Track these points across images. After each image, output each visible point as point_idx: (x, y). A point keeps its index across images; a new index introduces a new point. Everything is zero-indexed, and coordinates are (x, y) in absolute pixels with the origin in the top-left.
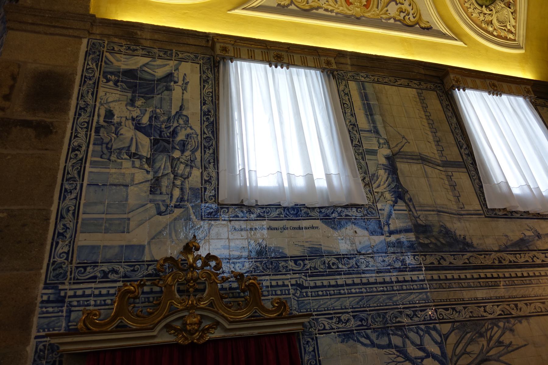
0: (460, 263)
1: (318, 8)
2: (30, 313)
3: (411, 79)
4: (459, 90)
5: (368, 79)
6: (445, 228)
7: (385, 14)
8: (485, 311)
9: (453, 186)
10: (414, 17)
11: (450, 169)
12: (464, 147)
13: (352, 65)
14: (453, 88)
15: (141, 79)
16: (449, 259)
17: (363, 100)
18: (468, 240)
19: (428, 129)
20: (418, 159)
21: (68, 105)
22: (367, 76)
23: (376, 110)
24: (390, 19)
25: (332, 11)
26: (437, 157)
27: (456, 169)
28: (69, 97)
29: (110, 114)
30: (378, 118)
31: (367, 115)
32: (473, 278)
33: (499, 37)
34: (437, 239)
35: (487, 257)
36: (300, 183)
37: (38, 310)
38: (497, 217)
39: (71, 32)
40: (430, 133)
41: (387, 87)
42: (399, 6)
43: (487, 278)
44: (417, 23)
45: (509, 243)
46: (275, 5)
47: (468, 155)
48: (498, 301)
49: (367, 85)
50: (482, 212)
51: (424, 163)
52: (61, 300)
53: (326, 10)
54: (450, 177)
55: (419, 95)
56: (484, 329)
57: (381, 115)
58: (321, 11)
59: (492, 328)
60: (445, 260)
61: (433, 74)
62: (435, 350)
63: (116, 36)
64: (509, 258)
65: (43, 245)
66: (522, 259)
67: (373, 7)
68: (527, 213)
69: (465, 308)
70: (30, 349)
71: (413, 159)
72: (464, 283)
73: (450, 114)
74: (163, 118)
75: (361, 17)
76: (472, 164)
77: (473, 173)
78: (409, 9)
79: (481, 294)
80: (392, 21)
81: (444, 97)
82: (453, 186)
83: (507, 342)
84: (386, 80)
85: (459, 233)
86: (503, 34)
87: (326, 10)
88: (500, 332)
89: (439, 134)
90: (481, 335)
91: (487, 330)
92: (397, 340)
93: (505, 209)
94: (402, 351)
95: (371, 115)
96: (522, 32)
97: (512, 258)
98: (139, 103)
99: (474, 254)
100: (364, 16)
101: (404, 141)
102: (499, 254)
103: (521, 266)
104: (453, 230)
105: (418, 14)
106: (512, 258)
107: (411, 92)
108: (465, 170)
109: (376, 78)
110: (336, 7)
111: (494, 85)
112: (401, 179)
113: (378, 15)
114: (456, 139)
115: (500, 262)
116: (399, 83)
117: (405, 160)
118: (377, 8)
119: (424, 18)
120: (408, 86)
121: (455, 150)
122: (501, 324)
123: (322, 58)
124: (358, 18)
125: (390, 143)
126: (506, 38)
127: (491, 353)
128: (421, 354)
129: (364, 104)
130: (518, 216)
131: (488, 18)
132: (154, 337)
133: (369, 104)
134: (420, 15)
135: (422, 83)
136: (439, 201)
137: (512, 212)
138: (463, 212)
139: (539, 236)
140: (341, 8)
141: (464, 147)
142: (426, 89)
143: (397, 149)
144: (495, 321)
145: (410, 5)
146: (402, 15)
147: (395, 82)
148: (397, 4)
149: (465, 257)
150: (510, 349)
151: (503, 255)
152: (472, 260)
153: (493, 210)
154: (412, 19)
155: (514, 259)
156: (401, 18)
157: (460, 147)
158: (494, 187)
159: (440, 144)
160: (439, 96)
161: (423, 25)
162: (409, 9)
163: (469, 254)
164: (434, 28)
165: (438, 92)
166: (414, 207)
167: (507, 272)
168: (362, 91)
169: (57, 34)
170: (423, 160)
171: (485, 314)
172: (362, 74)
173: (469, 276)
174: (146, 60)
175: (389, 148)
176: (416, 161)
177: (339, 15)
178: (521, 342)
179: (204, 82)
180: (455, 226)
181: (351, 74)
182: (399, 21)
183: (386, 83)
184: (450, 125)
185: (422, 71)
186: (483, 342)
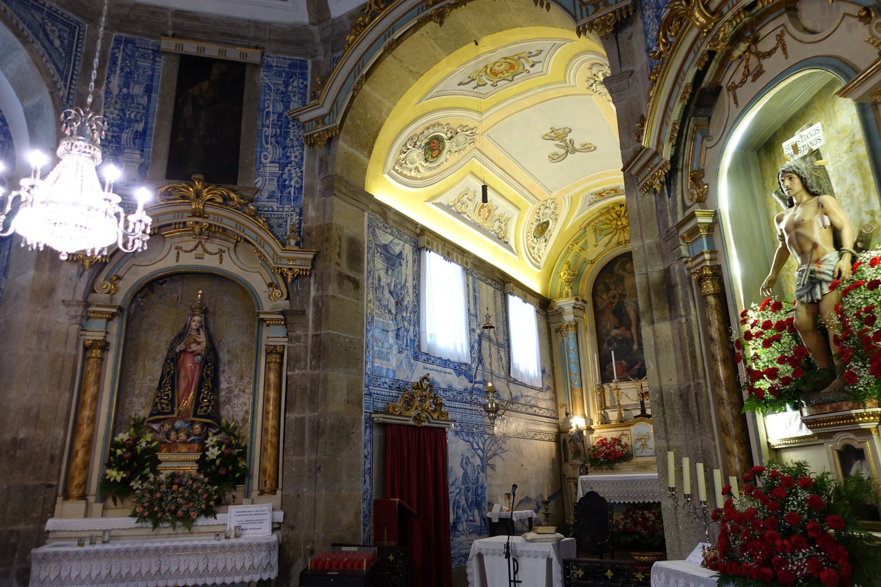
1: (465, 213)
2: (361, 399)
3: (493, 280)
15: (390, 254)
21: (363, 267)
23: (478, 303)
28: (363, 262)
29: (380, 280)
30: (478, 306)
33: (534, 258)
36: (451, 348)
37: (364, 399)
39: (360, 205)
46: (446, 204)
52: (370, 394)
53: (468, 216)
55: (495, 292)
58: (465, 216)
61: (502, 278)
62: (481, 446)
63: (378, 213)
65: (362, 362)
70: (363, 417)
74: (399, 287)
80: (493, 233)
84: (483, 278)
86: (537, 257)
87: (468, 216)
92: (471, 439)
94: (472, 445)
96: (544, 258)
98: (390, 272)
103: (513, 411)
105: (506, 233)
107: (491, 289)
111: (525, 296)
120: (491, 285)
123: (465, 259)
126: (536, 260)
128: (477, 447)
131: (534, 245)
132: (408, 421)
139: (522, 396)
161: (506, 240)
169: (356, 207)
174: (391, 238)
179: (414, 261)
183: (483, 281)
185: (499, 276)
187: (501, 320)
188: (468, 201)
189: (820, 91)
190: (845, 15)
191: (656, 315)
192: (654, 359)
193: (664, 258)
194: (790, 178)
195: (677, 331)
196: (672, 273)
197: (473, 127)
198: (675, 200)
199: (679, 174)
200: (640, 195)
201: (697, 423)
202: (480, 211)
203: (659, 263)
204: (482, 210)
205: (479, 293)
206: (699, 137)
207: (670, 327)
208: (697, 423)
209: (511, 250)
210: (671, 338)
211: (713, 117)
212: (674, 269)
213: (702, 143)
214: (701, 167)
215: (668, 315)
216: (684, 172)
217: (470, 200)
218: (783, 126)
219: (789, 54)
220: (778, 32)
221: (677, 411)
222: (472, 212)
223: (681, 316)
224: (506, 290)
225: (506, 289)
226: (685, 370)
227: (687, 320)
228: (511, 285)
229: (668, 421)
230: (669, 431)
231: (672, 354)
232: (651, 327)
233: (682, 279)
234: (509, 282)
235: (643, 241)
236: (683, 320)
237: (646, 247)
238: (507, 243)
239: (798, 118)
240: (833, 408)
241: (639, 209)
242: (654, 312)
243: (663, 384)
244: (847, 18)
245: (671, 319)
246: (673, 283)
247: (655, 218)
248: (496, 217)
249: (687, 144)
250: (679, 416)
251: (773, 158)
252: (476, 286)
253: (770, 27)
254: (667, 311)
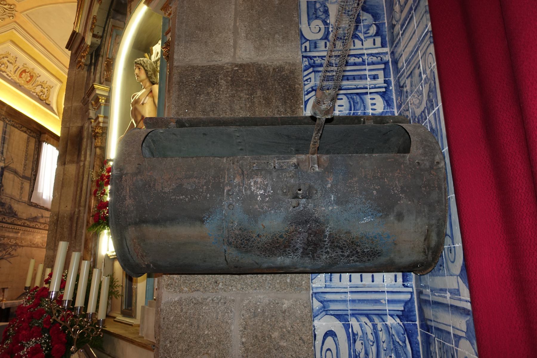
0: (9, 221)
3: (28, 129)
4: (46, 143)
5: (9, 123)
6: (11, 206)
7: (34, 89)
8: (10, 241)
9: (22, 188)
10: (46, 97)
11: (24, 180)
12: (34, 171)
13: (6, 112)
14: (44, 141)
16: (7, 219)
17: (3, 134)
18: (17, 213)
19: (24, 158)
20: (13, 172)
22: (10, 121)
23: (7, 142)
24: (34, 93)
25: (10, 77)
26: (22, 173)
27: (26, 181)
30: (6, 145)
31: (1, 143)
32: (11, 228)
34: (6, 210)
35: (20, 221)
38: (32, 206)
40: (24, 160)
41: (16, 130)
42: (42, 89)
43: (16, 229)
44: (45, 100)
45: (31, 217)
47: (34, 175)
48: (16, 239)
49: (8, 125)
50: (27, 202)
51: (16, 174)
53: (8, 75)
54: (22, 183)
55: (28, 138)
56: (6, 248)
57: (8, 145)
58: (4, 74)
59: (9, 248)
60: (5, 219)
61: (39, 129)
64: (28, 223)
66: (32, 224)
67: (30, 84)
68: (43, 207)
69: (4, 239)
71: (12, 171)
72: (8, 230)
73: (36, 153)
75: (22, 86)
76: (34, 180)
77: (32, 184)
78: (46, 92)
79: (11, 235)
80: (35, 94)
81: (37, 143)
82: (22, 188)
83: (12, 254)
84: (17, 126)
85: (15, 209)
87: (8, 75)
88: (11, 250)
89: (27, 162)
90: (5, 250)
91: (7, 249)
93: (36, 204)
95: (4, 143)
97: (28, 223)
99: (16, 219)
100: (23, 86)
101: (12, 161)
102: (25, 221)
104: (13, 207)
105: (48, 97)
106: (28, 223)
107: (25, 136)
108: (29, 182)
109: (14, 123)
110: (14, 75)
112: (3, 180)
113: (30, 88)
114: (33, 166)
115: (24, 224)
116: (22, 129)
117: (8, 171)
118: (32, 85)
119: (50, 99)
120: (25, 132)
121: (30, 171)
122: (13, 247)
124: (20, 86)
125: (6, 161)
127: (5, 257)
129: (2, 136)
130: (39, 207)
133: (4, 137)
134: (49, 97)
135: (32, 132)
136: (13, 194)
137: (38, 205)
138: (20, 201)
139: (42, 217)
140: (15, 77)
141: (34, 171)
142: (32, 136)
143: (7, 165)
144: (11, 246)
145: (47, 91)
146: (41, 93)
147: (20, 128)
148: (42, 87)
149: (13, 219)
150: (12, 256)
151: (27, 222)
152: (14, 221)
153: (32, 202)
154: (44, 97)
155: (29, 224)
156: (40, 94)
157: (32, 170)
158: (37, 193)
159: (26, 167)
160: (36, 142)
161: (47, 102)
162: (46, 92)
163: (14, 219)
164: (51, 105)
165: (37, 139)
166: (3, 194)
167: (24, 228)
168: (5, 129)
170: (15, 172)
171: (9, 243)
172: (8, 119)
173: (10, 227)
175: (4, 163)
176: (12, 172)
177: (12, 80)
178: (17, 255)
180: (15, 206)
181: (2, 117)
182: (38, 95)
183: (16, 127)
184: (34, 158)
186: (4, 252)
187: (31, 159)
188: (8, 64)
197: (11, 3)
202: (21, 74)
204: (24, 74)
205: (10, 136)
209: (52, 110)
217: (11, 63)
222: (12, 73)
224: (41, 139)
225: (41, 138)
228: (46, 135)
234: (45, 133)
235: (72, 104)
237: (73, 108)
238: (49, 105)
241: (75, 80)
247: (84, 89)
248: (39, 83)
249: (107, 38)
252: (8, 130)
254: (76, 156)
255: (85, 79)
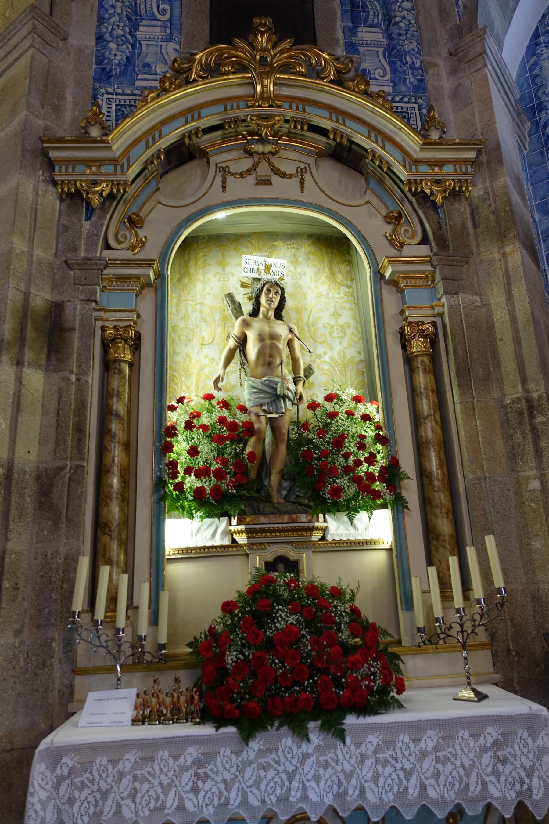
189: (260, 233)
190: (368, 202)
191: (29, 355)
192: (9, 416)
193: (55, 286)
194: (277, 293)
195: (55, 388)
196: (68, 311)
198: (98, 227)
199: (115, 203)
200: (42, 187)
201: (64, 519)
203: (47, 289)
206: (153, 186)
207: (42, 380)
208: (64, 519)
210: (41, 394)
211: (170, 176)
212: (75, 309)
213: (154, 193)
214: (142, 214)
215: (43, 362)
216: (119, 206)
218: (208, 236)
219: (305, 190)
220: (302, 166)
221: (28, 499)
223: (71, 372)
226: (57, 443)
227: (78, 380)
229: (13, 512)
230: (11, 527)
231: (38, 418)
232: (15, 369)
233: (82, 326)
235: (31, 248)
236: (73, 378)
237: (34, 258)
239: (228, 239)
240: (292, 519)
242: (27, 350)
243: (17, 455)
244: (369, 204)
245: (47, 370)
246: (67, 325)
249: (138, 180)
250: (30, 506)
251: (186, 257)
253: (294, 155)
254: (43, 356)
255: (57, 214)
